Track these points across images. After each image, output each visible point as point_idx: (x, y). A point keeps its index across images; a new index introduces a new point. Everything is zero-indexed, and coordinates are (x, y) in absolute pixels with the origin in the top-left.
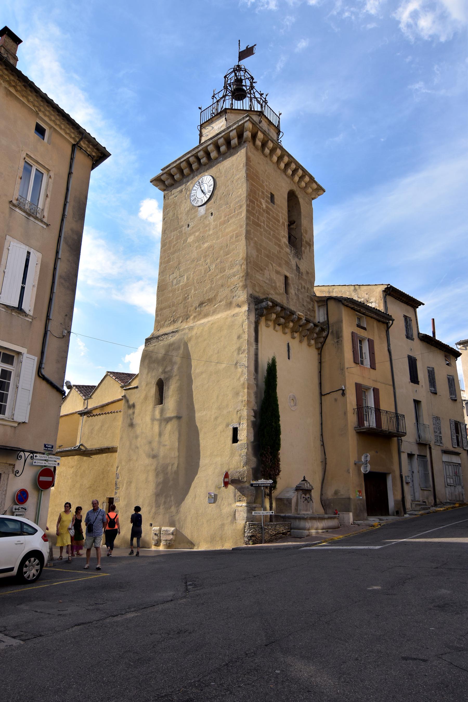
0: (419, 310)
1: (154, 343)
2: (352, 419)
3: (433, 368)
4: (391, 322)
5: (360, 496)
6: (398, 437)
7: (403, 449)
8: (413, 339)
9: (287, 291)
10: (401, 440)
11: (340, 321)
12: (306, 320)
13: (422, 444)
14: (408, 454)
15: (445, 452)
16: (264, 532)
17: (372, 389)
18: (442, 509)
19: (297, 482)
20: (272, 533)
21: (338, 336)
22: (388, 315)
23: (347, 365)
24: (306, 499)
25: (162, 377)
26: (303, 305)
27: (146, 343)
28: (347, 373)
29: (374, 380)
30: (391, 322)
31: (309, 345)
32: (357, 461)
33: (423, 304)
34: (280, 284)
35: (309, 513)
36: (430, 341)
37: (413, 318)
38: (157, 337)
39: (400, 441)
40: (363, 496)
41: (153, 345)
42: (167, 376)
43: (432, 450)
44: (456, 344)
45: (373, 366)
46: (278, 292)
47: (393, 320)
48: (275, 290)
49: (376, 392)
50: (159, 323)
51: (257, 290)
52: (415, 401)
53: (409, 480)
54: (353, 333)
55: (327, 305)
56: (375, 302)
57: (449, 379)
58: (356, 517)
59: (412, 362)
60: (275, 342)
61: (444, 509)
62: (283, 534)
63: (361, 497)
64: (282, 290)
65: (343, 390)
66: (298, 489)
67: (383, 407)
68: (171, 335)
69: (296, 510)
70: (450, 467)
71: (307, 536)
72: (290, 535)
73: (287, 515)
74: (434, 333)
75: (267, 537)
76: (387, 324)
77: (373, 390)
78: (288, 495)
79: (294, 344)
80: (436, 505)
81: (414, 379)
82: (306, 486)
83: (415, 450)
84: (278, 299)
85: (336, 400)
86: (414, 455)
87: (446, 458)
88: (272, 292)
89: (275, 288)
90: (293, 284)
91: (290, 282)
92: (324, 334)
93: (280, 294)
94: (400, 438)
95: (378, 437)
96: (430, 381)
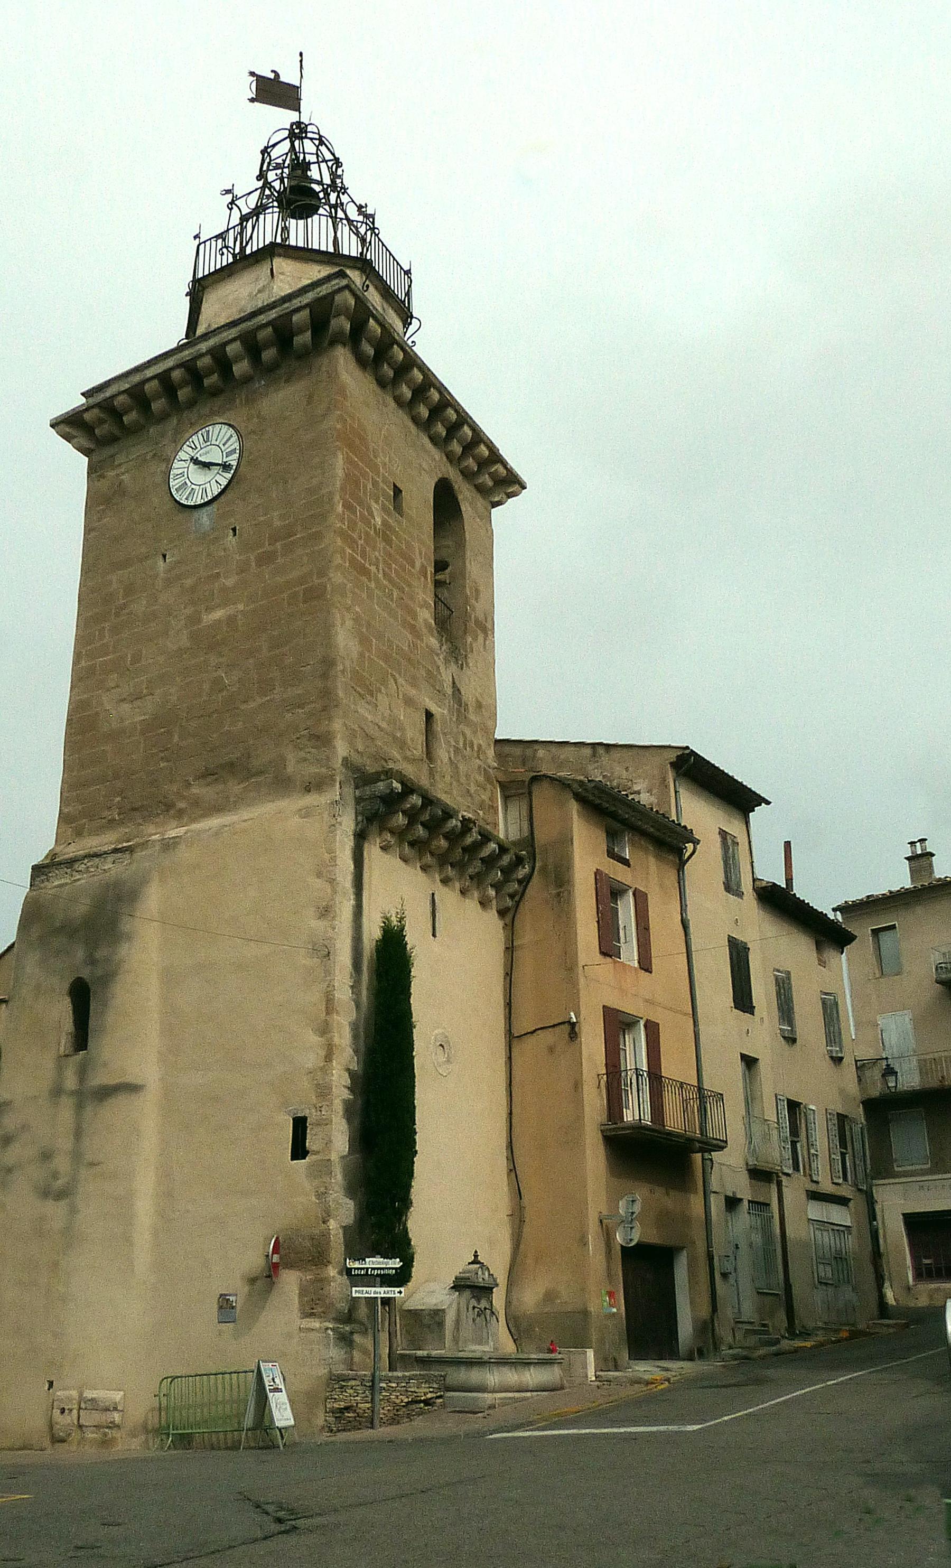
0: (757, 815)
1: (58, 880)
2: (594, 1102)
3: (788, 973)
4: (690, 846)
5: (611, 1306)
6: (702, 1150)
7: (714, 1184)
8: (740, 894)
9: (429, 754)
10: (711, 1160)
11: (566, 841)
12: (480, 834)
13: (760, 1175)
14: (727, 1198)
15: (815, 1196)
16: (378, 1397)
17: (642, 1023)
18: (808, 1344)
19: (459, 1265)
20: (398, 1401)
21: (561, 880)
22: (685, 827)
23: (582, 959)
24: (481, 1313)
25: (85, 973)
26: (468, 791)
27: (33, 878)
28: (582, 981)
29: (647, 1001)
30: (690, 846)
31: (484, 903)
32: (605, 1213)
33: (768, 803)
34: (414, 733)
35: (486, 1348)
36: (779, 901)
37: (742, 839)
38: (71, 863)
39: (708, 1162)
40: (619, 1308)
41: (56, 883)
42: (99, 972)
43: (785, 1190)
44: (834, 910)
45: (645, 965)
46: (409, 753)
47: (696, 842)
48: (401, 748)
49: (652, 1030)
50: (72, 819)
51: (361, 748)
52: (744, 1057)
53: (729, 1267)
54: (598, 873)
55: (530, 793)
56: (650, 791)
57: (824, 1002)
58: (607, 1362)
59: (739, 955)
60: (398, 888)
61: (813, 1343)
62: (427, 1402)
63: (615, 1310)
64: (419, 750)
65: (573, 1025)
66: (459, 1285)
67: (668, 1069)
68: (110, 859)
69: (456, 1340)
70: (825, 1233)
71: (490, 1408)
72: (443, 1406)
73: (434, 1353)
74: (789, 880)
75: (383, 1411)
76: (679, 852)
77: (645, 1026)
78: (434, 1301)
79: (448, 898)
80: (792, 1333)
81: (743, 1000)
82: (482, 1278)
83: (742, 1187)
84: (409, 770)
85: (551, 1050)
86: (741, 1200)
87: (816, 1211)
88: (395, 754)
89: (402, 744)
90: (445, 734)
91: (438, 727)
92: (522, 872)
93: (414, 760)
94: (707, 1156)
95: (654, 1155)
96: (780, 1008)
